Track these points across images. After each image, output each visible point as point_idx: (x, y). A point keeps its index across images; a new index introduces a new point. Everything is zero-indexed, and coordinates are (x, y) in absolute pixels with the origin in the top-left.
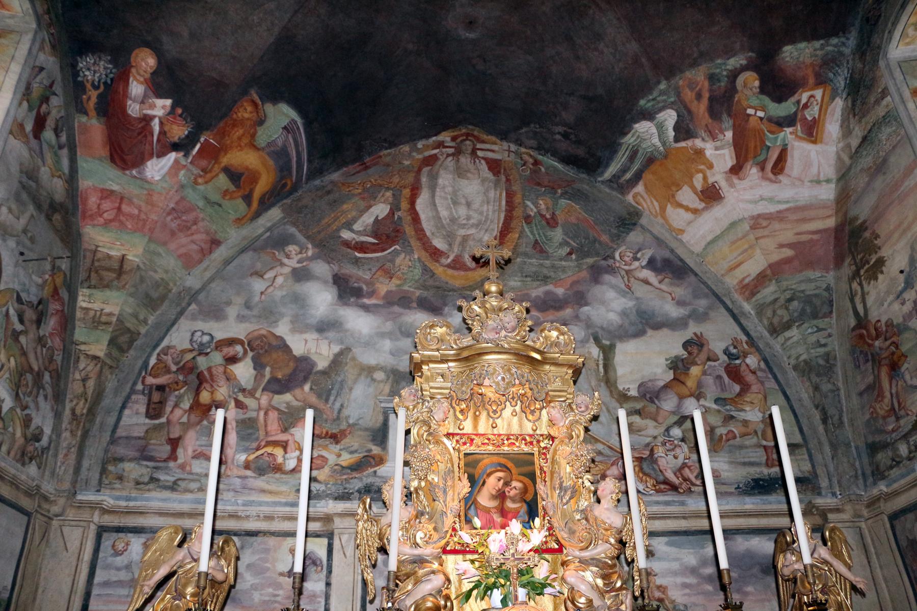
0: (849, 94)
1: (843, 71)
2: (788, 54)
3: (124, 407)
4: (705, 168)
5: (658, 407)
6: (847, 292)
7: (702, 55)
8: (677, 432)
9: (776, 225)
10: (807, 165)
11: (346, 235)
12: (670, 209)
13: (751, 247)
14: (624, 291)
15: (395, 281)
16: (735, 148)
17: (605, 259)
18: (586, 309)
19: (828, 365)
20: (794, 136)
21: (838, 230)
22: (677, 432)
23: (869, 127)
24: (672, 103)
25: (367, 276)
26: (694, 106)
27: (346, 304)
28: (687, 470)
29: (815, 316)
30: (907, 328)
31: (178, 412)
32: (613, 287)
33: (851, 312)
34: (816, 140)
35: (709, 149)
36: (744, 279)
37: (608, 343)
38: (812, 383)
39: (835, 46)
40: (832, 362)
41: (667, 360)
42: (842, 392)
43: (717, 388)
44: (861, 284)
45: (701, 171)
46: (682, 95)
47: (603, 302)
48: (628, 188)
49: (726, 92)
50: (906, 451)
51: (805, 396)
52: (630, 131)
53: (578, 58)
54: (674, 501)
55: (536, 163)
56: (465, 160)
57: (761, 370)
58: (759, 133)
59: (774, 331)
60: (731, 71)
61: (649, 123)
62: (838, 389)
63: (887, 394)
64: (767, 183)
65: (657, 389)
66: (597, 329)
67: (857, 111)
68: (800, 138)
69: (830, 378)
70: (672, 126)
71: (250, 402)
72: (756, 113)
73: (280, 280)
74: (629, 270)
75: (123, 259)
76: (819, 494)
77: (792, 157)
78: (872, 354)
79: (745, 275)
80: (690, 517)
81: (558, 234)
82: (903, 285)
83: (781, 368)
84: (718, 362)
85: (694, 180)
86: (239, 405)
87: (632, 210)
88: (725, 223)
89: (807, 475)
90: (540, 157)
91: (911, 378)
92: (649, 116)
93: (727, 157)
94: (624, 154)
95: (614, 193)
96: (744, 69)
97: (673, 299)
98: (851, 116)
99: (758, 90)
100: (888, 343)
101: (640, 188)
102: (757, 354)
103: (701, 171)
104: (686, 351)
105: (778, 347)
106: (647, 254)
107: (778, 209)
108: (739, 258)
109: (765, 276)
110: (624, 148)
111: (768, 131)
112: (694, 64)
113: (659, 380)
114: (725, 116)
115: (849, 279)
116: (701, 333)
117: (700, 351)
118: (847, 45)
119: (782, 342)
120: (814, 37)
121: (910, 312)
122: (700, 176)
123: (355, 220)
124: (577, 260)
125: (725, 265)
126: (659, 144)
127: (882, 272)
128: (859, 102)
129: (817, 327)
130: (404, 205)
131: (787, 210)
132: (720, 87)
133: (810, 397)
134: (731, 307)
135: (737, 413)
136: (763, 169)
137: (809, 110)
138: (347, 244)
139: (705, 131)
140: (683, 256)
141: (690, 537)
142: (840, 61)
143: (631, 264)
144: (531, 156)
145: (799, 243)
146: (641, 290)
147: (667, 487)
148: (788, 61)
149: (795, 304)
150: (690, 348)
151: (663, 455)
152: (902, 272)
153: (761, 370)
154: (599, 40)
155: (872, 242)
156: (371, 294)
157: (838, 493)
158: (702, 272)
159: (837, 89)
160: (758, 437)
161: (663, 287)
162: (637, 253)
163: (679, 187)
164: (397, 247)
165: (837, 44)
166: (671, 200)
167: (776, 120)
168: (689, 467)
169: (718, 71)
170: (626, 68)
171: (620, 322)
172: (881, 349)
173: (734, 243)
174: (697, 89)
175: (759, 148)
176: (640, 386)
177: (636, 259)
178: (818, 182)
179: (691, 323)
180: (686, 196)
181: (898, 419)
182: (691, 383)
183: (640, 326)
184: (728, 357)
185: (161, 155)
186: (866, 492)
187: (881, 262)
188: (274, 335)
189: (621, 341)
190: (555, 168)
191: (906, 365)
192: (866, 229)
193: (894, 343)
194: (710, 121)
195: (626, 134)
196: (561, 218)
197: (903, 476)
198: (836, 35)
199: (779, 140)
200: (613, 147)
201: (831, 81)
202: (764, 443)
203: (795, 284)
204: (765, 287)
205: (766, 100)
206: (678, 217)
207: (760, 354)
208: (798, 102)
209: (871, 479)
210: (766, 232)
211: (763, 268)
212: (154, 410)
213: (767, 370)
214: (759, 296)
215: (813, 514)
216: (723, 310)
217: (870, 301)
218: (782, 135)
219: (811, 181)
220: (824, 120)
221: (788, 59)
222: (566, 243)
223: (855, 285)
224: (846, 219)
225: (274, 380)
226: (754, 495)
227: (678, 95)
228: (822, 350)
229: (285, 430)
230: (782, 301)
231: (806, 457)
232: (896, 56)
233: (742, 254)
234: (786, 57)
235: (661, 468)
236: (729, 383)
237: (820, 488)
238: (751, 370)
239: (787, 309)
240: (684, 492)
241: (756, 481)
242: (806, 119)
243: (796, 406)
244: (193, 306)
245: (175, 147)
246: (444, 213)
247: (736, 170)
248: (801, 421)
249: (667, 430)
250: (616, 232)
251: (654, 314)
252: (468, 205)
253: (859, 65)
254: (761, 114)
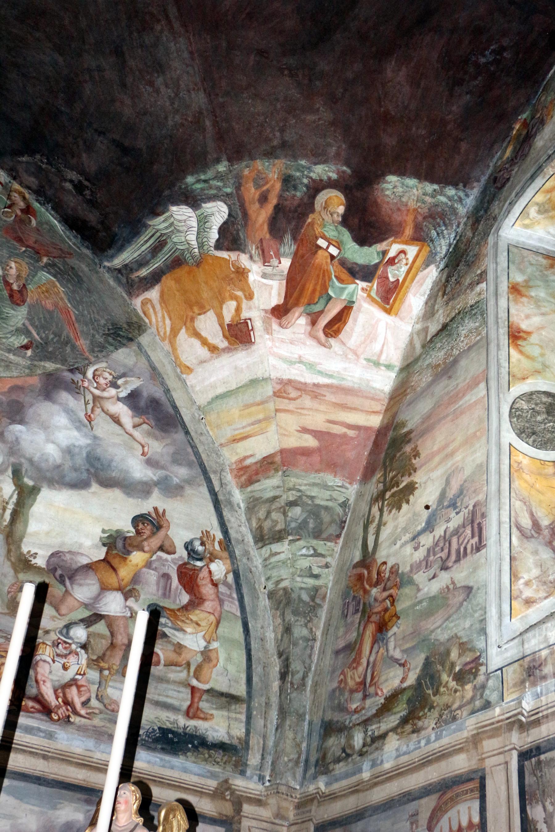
0: (447, 266)
1: (449, 234)
2: (390, 186)
4: (243, 297)
5: (67, 591)
6: (363, 516)
7: (284, 145)
9: (307, 401)
10: (370, 338)
12: (183, 334)
13: (267, 419)
14: (80, 421)
16: (287, 283)
17: (71, 371)
18: (18, 428)
19: (311, 603)
20: (365, 295)
21: (382, 432)
23: (453, 314)
24: (228, 194)
26: (253, 208)
28: (74, 689)
29: (317, 534)
30: (411, 582)
32: (69, 412)
33: (360, 543)
34: (391, 309)
36: (245, 458)
37: (31, 483)
38: (284, 620)
39: (450, 198)
40: (318, 601)
41: (104, 531)
42: (318, 644)
43: (158, 590)
44: (381, 510)
45: (236, 298)
46: (242, 188)
47: (45, 427)
48: (139, 288)
49: (299, 206)
50: (361, 742)
51: (270, 635)
52: (163, 213)
53: (123, 85)
54: (39, 729)
55: (28, 210)
57: (225, 583)
58: (324, 276)
60: (314, 181)
61: (190, 210)
62: (314, 640)
63: (364, 661)
64: (313, 343)
65: (74, 567)
66: (23, 460)
67: (448, 289)
68: (373, 300)
69: (309, 621)
70: (219, 225)
72: (328, 247)
74: (99, 397)
76: (243, 773)
77: (355, 320)
78: (364, 604)
79: (249, 454)
80: (53, 758)
82: (423, 524)
83: (253, 590)
84: (173, 556)
85: (224, 307)
87: (135, 319)
88: (245, 378)
89: (235, 742)
90: (36, 205)
91: (395, 648)
93: (274, 292)
94: (147, 241)
95: (120, 290)
96: (331, 184)
97: (143, 454)
98: (440, 294)
99: (340, 219)
100: (386, 594)
101: (154, 294)
102: (228, 561)
103: (236, 298)
104: (135, 527)
105: (258, 561)
106: (133, 384)
107: (316, 381)
108: (248, 429)
109: (272, 463)
110: (149, 232)
111: (335, 276)
112: (270, 154)
113: (82, 554)
114: (288, 238)
115: (371, 499)
116: (164, 510)
117: (153, 534)
118: (464, 202)
119: (267, 555)
121: (420, 562)
122: (233, 304)
124: (31, 358)
125: (228, 433)
126: (194, 243)
127: (408, 502)
128: (453, 279)
129: (315, 550)
131: (327, 386)
132: (294, 196)
133: (276, 639)
134: (217, 489)
135: (172, 631)
136: (313, 323)
137: (393, 267)
139: (257, 248)
140: (179, 403)
141: (43, 789)
142: (450, 220)
143: (104, 390)
144: (24, 198)
145: (328, 433)
147: (37, 706)
148: (387, 196)
149: (297, 511)
150: (141, 526)
151: (49, 660)
152: (427, 507)
153: (225, 583)
154: (158, 72)
155: (410, 460)
157: (268, 778)
158: (196, 432)
159: (436, 254)
160: (189, 672)
161: (137, 434)
162: (120, 377)
163: (203, 310)
165: (453, 196)
166: (188, 324)
167: (350, 266)
168: (79, 687)
169: (298, 174)
170: (182, 125)
171: (59, 461)
172: (376, 600)
173: (247, 406)
174: (265, 188)
175: (317, 294)
176: (53, 555)
177: (114, 385)
178: (377, 364)
179: (156, 493)
181: (365, 697)
182: (125, 573)
183: (85, 476)
184: (189, 554)
186: (302, 785)
187: (411, 488)
189: (49, 487)
190: (52, 228)
191: (395, 629)
192: (409, 441)
193: (391, 596)
194: (268, 236)
195: (158, 215)
196: (32, 296)
197: (347, 775)
198: (455, 185)
199: (346, 292)
201: (432, 241)
202: (194, 682)
203: (306, 485)
204: (268, 477)
205: (346, 236)
207: (233, 563)
208: (385, 253)
209: (312, 770)
210: (291, 406)
211: (272, 451)
213: (234, 586)
214: (256, 486)
215: (224, 798)
216: (204, 490)
217: (385, 533)
218: (353, 286)
219: (368, 360)
220: (408, 287)
221: (387, 193)
222: (27, 333)
223: (375, 510)
224: (393, 422)
226: (154, 750)
227: (238, 187)
228: (311, 582)
230: (282, 502)
231: (243, 717)
232: (509, 237)
233: (253, 424)
234: (388, 189)
235: (39, 677)
236: (177, 588)
237: (246, 765)
238: (212, 580)
239: (285, 514)
240: (59, 719)
241: (164, 731)
242: (387, 278)
243: (254, 645)
248: (254, 666)
249: (68, 627)
250: (102, 340)
251: (109, 466)
253: (469, 234)
254: (333, 251)
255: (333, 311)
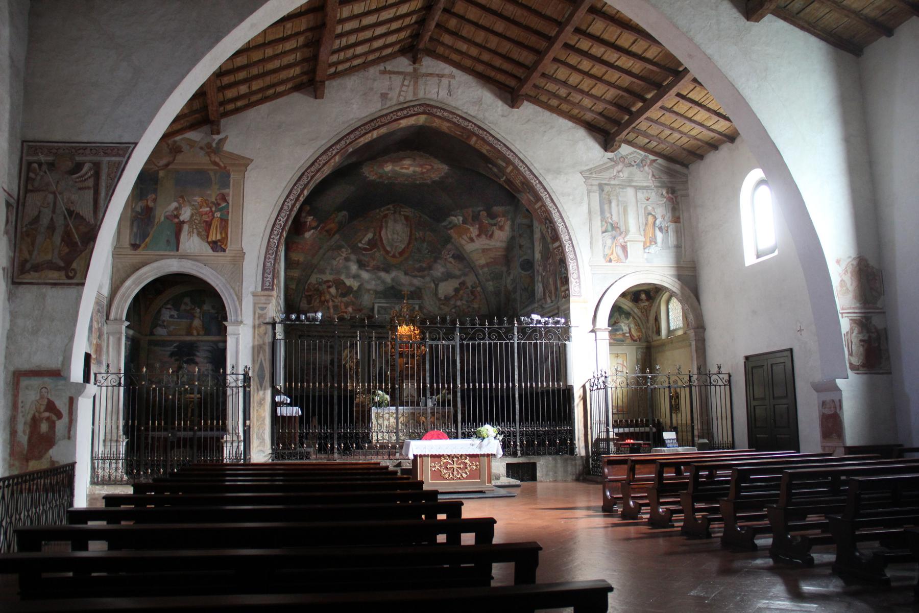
3: (300, 302)
8: (453, 310)
11: (360, 245)
15: (375, 262)
18: (432, 272)
22: (453, 310)
25: (367, 259)
27: (361, 269)
31: (316, 303)
35: (471, 229)
56: (397, 215)
59: (487, 280)
71: (334, 300)
73: (341, 261)
75: (298, 261)
81: (425, 245)
86: (333, 301)
92: (456, 216)
101: (452, 231)
106: (452, 253)
120: (503, 205)
123: (362, 239)
130: (378, 234)
136: (486, 236)
138: (360, 248)
146: (448, 265)
156: (368, 266)
164: (376, 250)
180: (465, 237)
182: (460, 296)
185: (309, 231)
188: (340, 279)
200: (444, 220)
205: (489, 219)
206: (463, 242)
212: (309, 303)
225: (342, 293)
229: (346, 308)
244: (316, 270)
245: (313, 228)
246: (390, 237)
247: (479, 236)
252: (398, 234)
255: (490, 233)
